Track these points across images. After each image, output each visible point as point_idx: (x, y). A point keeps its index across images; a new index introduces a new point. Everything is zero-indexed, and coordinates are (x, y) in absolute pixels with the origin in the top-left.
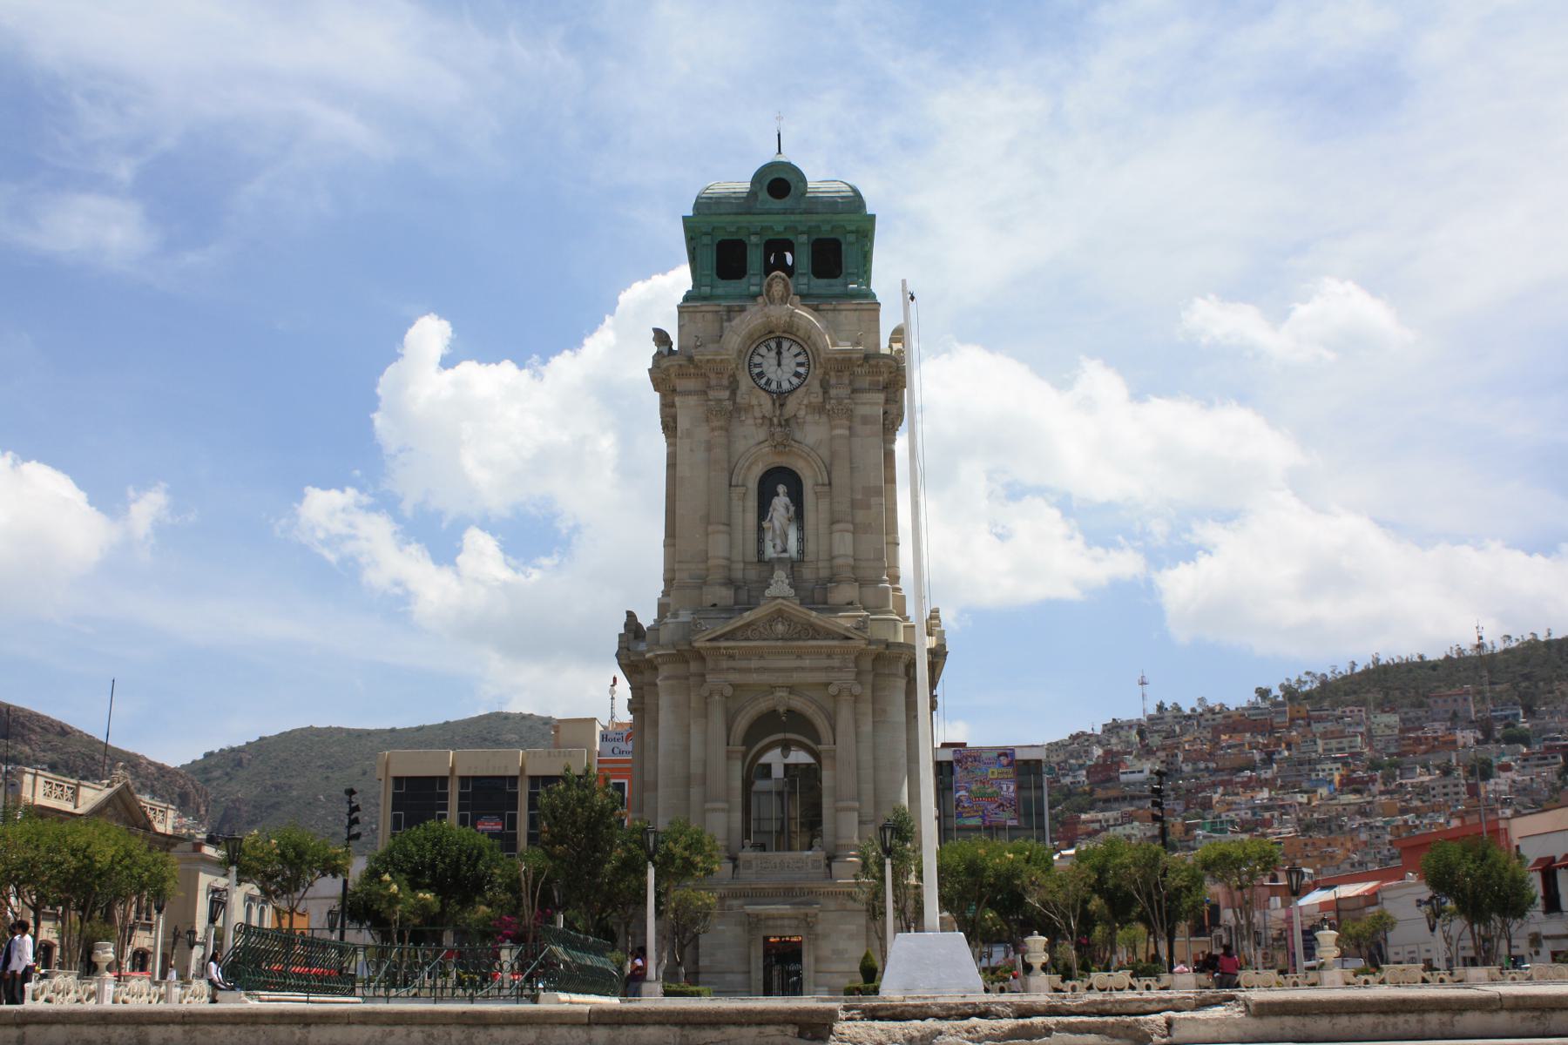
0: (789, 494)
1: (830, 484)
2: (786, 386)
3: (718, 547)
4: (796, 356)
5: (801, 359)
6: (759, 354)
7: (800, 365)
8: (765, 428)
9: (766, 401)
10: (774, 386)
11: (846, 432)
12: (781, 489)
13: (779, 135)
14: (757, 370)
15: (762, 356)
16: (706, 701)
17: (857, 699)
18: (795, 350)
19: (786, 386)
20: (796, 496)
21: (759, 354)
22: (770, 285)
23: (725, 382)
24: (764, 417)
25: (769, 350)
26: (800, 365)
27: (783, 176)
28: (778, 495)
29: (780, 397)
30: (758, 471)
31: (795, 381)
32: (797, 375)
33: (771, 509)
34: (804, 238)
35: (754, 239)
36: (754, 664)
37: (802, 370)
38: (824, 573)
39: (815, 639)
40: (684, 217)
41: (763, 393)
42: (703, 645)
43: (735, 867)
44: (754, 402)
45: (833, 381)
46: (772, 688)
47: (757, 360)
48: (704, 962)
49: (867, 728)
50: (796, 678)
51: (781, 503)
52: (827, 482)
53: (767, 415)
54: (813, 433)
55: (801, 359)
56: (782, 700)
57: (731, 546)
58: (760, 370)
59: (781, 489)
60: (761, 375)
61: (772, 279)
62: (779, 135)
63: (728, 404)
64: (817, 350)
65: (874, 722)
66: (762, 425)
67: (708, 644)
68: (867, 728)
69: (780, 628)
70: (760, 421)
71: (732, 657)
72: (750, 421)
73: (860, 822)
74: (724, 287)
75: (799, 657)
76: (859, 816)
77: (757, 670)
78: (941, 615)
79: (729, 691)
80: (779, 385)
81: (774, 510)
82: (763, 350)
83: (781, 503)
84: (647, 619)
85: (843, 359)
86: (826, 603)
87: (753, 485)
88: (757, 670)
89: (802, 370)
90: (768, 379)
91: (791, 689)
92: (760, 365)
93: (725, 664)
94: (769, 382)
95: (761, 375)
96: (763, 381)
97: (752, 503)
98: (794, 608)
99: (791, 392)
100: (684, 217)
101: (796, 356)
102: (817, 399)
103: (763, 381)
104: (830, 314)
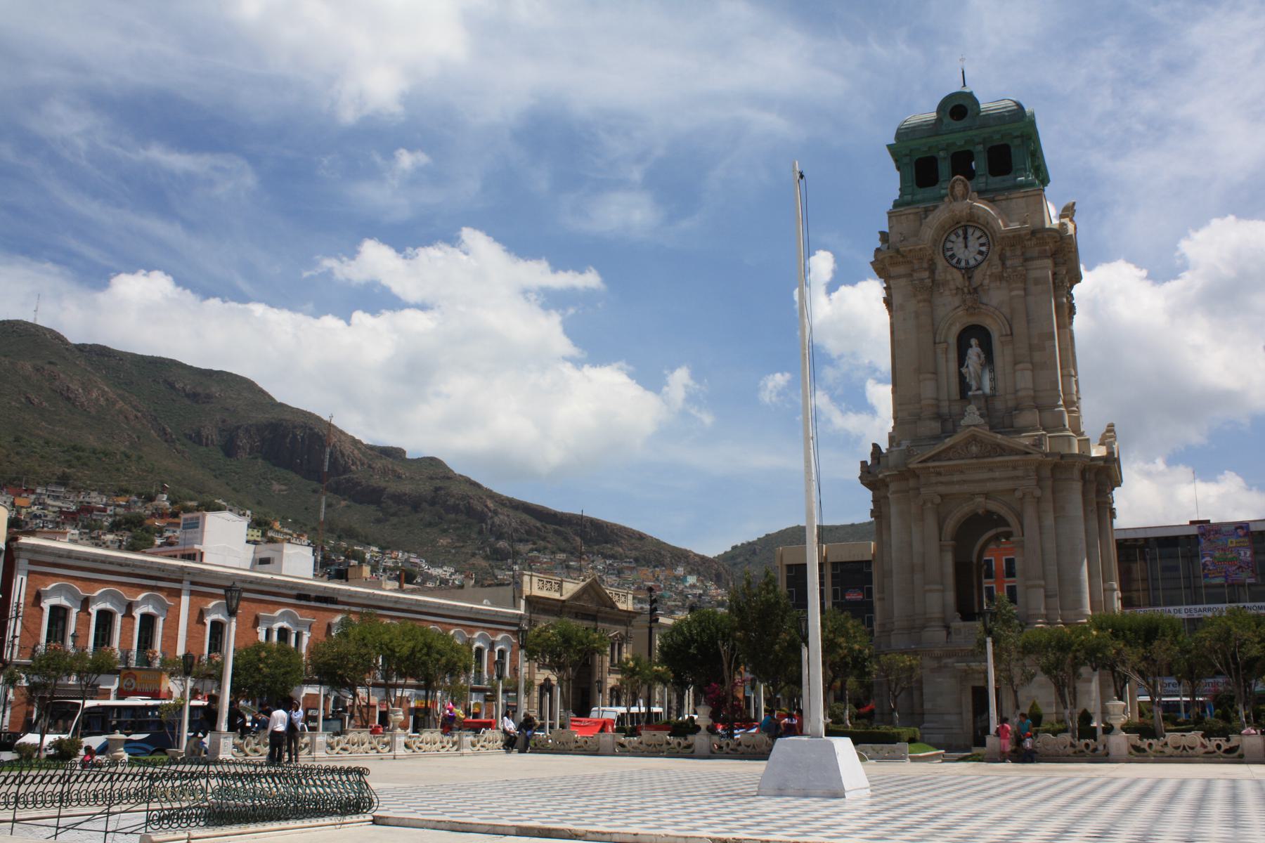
0: (980, 345)
1: (1012, 334)
2: (972, 262)
3: (928, 390)
4: (979, 238)
5: (983, 240)
6: (950, 241)
7: (982, 245)
9: (957, 275)
10: (963, 264)
11: (1022, 293)
12: (974, 342)
13: (963, 72)
14: (949, 253)
17: (1039, 500)
18: (978, 234)
19: (972, 262)
21: (950, 241)
22: (953, 187)
23: (925, 265)
24: (957, 288)
25: (958, 236)
27: (961, 102)
28: (971, 347)
29: (968, 271)
30: (956, 329)
31: (979, 258)
32: (981, 253)
34: (980, 147)
35: (942, 154)
36: (956, 478)
37: (984, 249)
38: (1011, 404)
39: (1001, 455)
40: (888, 146)
41: (955, 270)
43: (949, 633)
44: (949, 277)
45: (1008, 254)
46: (973, 495)
47: (949, 245)
48: (927, 706)
49: (1049, 520)
50: (989, 486)
51: (974, 353)
52: (1009, 332)
53: (959, 286)
54: (996, 296)
55: (983, 240)
56: (980, 504)
57: (938, 389)
59: (974, 342)
60: (952, 256)
61: (954, 182)
62: (963, 72)
63: (928, 282)
64: (995, 231)
65: (1055, 518)
66: (956, 294)
67: (920, 465)
68: (1049, 520)
69: (974, 449)
70: (955, 292)
71: (939, 474)
72: (947, 293)
73: (1046, 596)
75: (991, 470)
76: (1045, 592)
77: (958, 482)
78: (1116, 429)
79: (938, 500)
80: (967, 262)
82: (953, 237)
83: (974, 353)
84: (884, 446)
85: (1014, 237)
86: (1012, 427)
87: (953, 340)
88: (958, 482)
89: (984, 249)
90: (959, 259)
91: (987, 495)
92: (951, 249)
93: (934, 479)
94: (959, 261)
95: (952, 256)
96: (955, 261)
97: (953, 355)
98: (985, 433)
99: (976, 267)
100: (888, 146)
101: (979, 238)
102: (997, 269)
103: (955, 261)
104: (1004, 203)
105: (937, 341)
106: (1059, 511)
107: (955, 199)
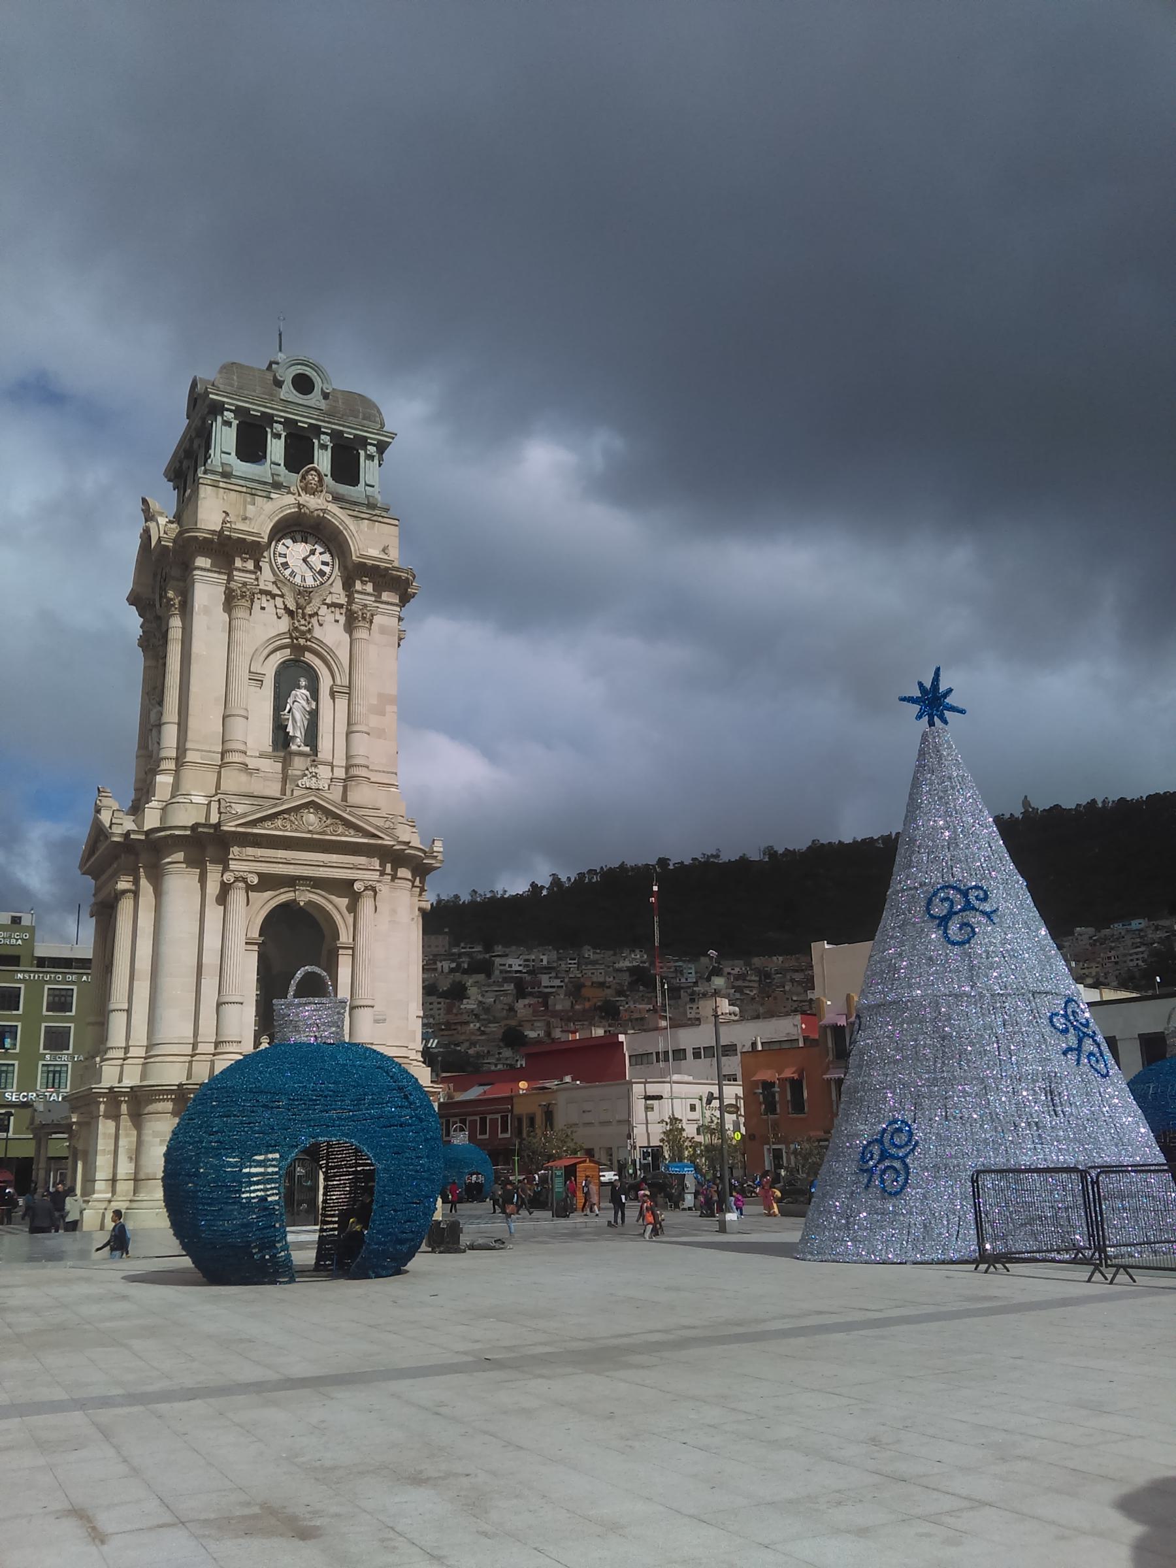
1: (349, 687)
6: (283, 544)
7: (324, 563)
8: (286, 619)
12: (303, 683)
13: (280, 335)
14: (281, 560)
15: (288, 547)
16: (225, 888)
20: (315, 694)
21: (283, 544)
24: (286, 608)
26: (324, 563)
28: (299, 688)
33: (290, 701)
41: (287, 582)
42: (233, 829)
56: (304, 896)
58: (284, 560)
59: (303, 683)
61: (307, 472)
62: (280, 335)
74: (242, 468)
79: (255, 880)
80: (304, 579)
81: (295, 701)
90: (293, 572)
92: (285, 556)
93: (250, 851)
103: (287, 572)
105: (252, 670)
106: (394, 911)
107: (306, 489)
